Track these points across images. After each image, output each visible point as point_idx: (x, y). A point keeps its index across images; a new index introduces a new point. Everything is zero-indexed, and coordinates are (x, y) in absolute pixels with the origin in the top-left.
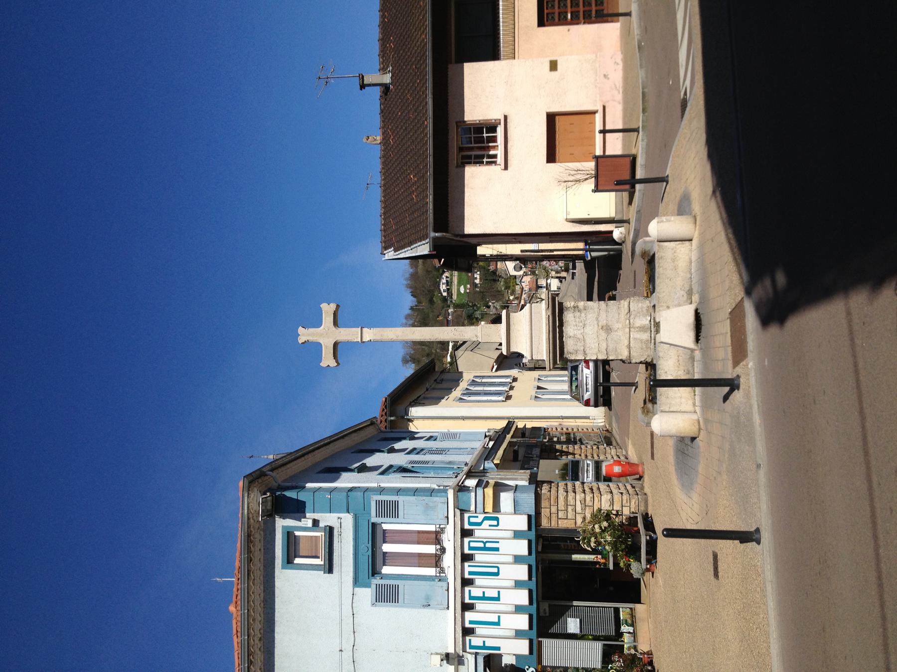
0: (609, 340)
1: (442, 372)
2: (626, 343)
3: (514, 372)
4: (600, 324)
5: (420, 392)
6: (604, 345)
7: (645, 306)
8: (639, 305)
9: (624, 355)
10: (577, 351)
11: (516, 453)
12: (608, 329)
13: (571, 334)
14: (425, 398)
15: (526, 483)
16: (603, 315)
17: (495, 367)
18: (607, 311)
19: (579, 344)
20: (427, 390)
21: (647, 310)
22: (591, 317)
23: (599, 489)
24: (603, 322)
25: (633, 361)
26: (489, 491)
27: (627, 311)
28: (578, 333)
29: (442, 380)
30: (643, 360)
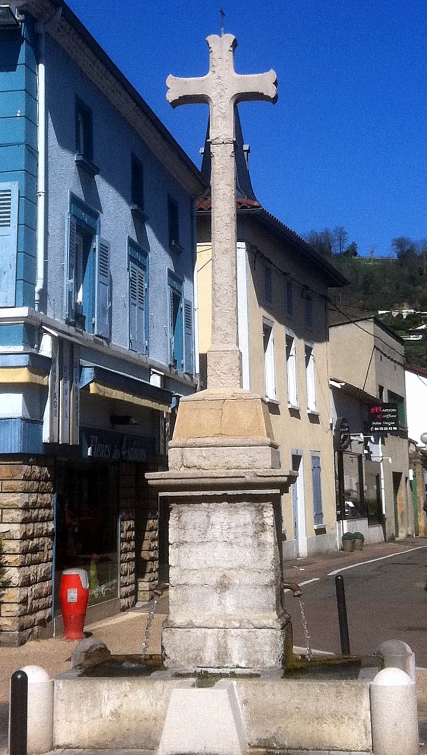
1: (326, 299)
2: (198, 621)
3: (330, 416)
4: (234, 573)
5: (279, 261)
6: (194, 579)
8: (268, 647)
9: (178, 618)
10: (183, 528)
11: (125, 420)
12: (223, 586)
14: (267, 270)
15: (46, 437)
16: (248, 579)
17: (338, 385)
18: (255, 586)
19: (196, 533)
20: (285, 274)
21: (258, 661)
22: (245, 554)
23: (38, 562)
24: (238, 578)
26: (23, 376)
29: (309, 298)
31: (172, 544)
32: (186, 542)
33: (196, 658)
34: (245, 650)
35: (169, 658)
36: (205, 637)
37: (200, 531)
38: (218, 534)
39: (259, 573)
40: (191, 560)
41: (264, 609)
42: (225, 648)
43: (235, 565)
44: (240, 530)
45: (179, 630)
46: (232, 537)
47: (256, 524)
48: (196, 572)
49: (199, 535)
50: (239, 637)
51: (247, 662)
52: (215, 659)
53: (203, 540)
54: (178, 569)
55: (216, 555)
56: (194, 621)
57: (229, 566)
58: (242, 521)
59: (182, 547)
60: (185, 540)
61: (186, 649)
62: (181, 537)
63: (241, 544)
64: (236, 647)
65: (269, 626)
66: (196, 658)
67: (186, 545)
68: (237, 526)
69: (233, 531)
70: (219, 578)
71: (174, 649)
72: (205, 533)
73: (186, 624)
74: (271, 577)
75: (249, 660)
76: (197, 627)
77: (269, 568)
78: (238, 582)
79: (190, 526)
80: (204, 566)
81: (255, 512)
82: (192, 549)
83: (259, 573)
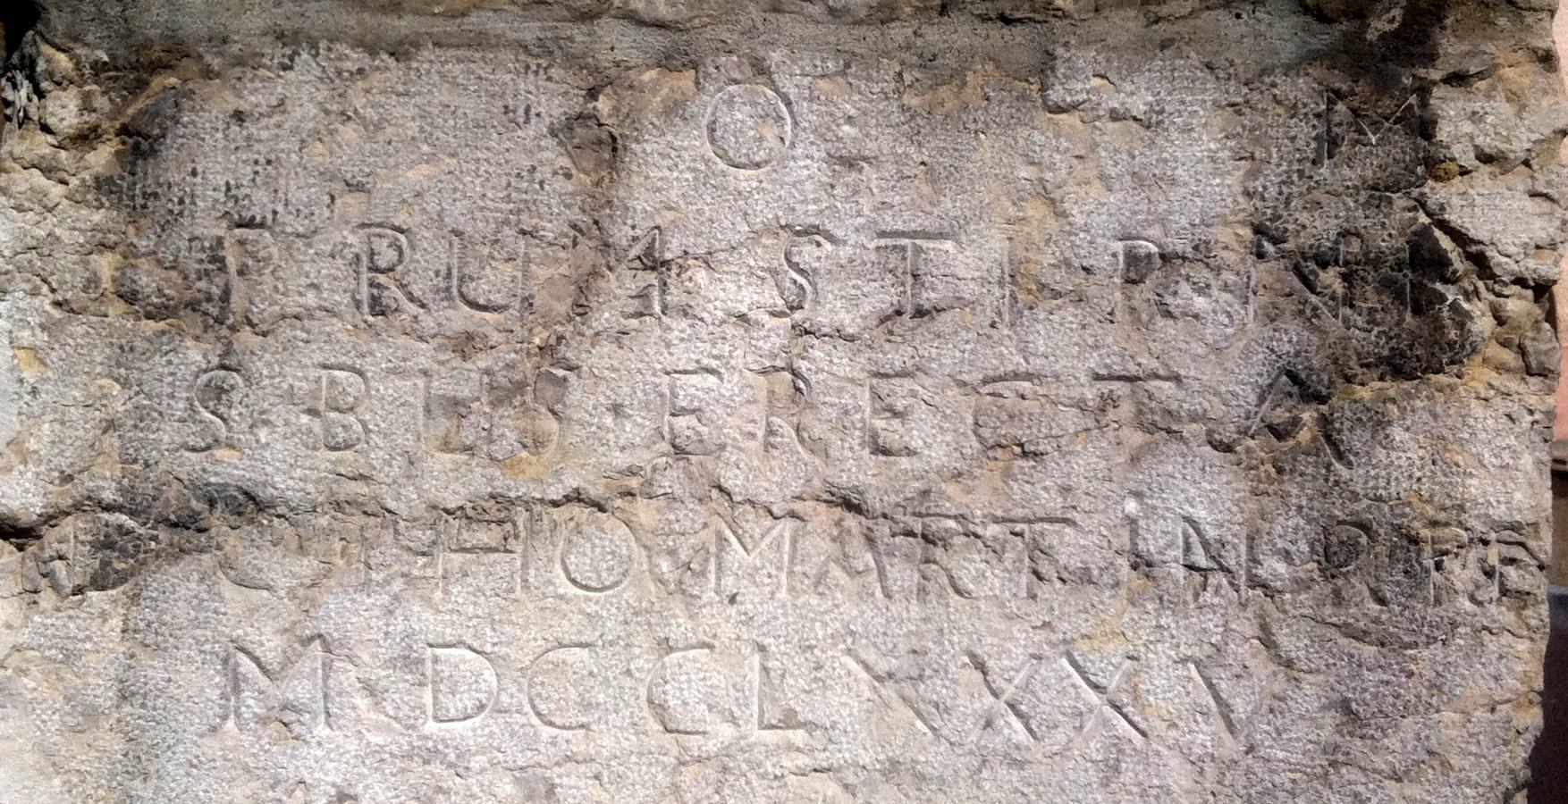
13: (669, 178)
28: (700, 361)
32: (249, 505)
37: (466, 344)
44: (1065, 347)
46: (933, 441)
47: (1307, 265)
49: (456, 407)
55: (693, 682)
58: (1100, 217)
59: (178, 586)
60: (229, 468)
63: (1069, 546)
67: (232, 539)
68: (1025, 289)
69: (951, 351)
79: (310, 277)
81: (1300, 88)
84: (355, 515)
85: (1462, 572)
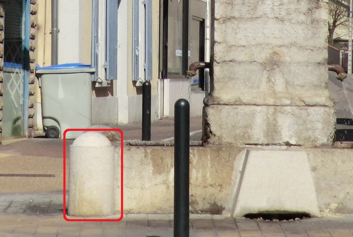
0: (254, 67)
2: (246, 98)
4: (284, 50)
6: (240, 56)
7: (318, 134)
16: (301, 56)
18: (307, 64)
22: (297, 32)
24: (288, 55)
25: (210, 111)
27: (308, 101)
30: (213, 128)
31: (217, 20)
32: (234, 18)
33: (244, 135)
34: (296, 127)
35: (215, 135)
36: (254, 114)
37: (249, 6)
38: (268, 10)
39: (312, 50)
40: (239, 36)
41: (316, 87)
42: (275, 125)
43: (287, 41)
45: (227, 107)
46: (283, 13)
48: (243, 48)
49: (248, 11)
50: (289, 115)
51: (297, 139)
52: (264, 137)
53: (253, 16)
54: (224, 45)
56: (241, 98)
57: (280, 42)
59: (229, 24)
60: (233, 15)
61: (233, 126)
62: (228, 13)
64: (287, 124)
65: (322, 103)
66: (244, 135)
67: (233, 20)
69: (285, 7)
70: (268, 55)
71: (221, 127)
72: (255, 8)
73: (233, 100)
74: (325, 55)
75: (299, 137)
76: (245, 104)
77: (323, 45)
78: (288, 59)
80: (253, 43)
82: (240, 25)
83: (312, 50)
84: (241, 19)
85: (322, 23)
